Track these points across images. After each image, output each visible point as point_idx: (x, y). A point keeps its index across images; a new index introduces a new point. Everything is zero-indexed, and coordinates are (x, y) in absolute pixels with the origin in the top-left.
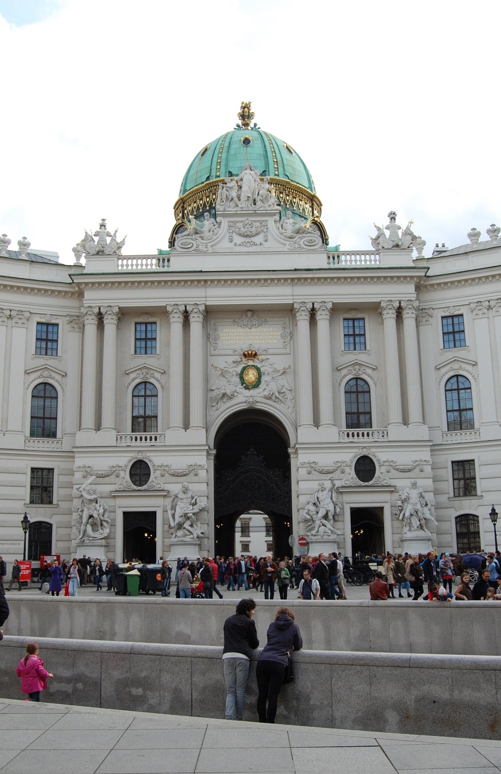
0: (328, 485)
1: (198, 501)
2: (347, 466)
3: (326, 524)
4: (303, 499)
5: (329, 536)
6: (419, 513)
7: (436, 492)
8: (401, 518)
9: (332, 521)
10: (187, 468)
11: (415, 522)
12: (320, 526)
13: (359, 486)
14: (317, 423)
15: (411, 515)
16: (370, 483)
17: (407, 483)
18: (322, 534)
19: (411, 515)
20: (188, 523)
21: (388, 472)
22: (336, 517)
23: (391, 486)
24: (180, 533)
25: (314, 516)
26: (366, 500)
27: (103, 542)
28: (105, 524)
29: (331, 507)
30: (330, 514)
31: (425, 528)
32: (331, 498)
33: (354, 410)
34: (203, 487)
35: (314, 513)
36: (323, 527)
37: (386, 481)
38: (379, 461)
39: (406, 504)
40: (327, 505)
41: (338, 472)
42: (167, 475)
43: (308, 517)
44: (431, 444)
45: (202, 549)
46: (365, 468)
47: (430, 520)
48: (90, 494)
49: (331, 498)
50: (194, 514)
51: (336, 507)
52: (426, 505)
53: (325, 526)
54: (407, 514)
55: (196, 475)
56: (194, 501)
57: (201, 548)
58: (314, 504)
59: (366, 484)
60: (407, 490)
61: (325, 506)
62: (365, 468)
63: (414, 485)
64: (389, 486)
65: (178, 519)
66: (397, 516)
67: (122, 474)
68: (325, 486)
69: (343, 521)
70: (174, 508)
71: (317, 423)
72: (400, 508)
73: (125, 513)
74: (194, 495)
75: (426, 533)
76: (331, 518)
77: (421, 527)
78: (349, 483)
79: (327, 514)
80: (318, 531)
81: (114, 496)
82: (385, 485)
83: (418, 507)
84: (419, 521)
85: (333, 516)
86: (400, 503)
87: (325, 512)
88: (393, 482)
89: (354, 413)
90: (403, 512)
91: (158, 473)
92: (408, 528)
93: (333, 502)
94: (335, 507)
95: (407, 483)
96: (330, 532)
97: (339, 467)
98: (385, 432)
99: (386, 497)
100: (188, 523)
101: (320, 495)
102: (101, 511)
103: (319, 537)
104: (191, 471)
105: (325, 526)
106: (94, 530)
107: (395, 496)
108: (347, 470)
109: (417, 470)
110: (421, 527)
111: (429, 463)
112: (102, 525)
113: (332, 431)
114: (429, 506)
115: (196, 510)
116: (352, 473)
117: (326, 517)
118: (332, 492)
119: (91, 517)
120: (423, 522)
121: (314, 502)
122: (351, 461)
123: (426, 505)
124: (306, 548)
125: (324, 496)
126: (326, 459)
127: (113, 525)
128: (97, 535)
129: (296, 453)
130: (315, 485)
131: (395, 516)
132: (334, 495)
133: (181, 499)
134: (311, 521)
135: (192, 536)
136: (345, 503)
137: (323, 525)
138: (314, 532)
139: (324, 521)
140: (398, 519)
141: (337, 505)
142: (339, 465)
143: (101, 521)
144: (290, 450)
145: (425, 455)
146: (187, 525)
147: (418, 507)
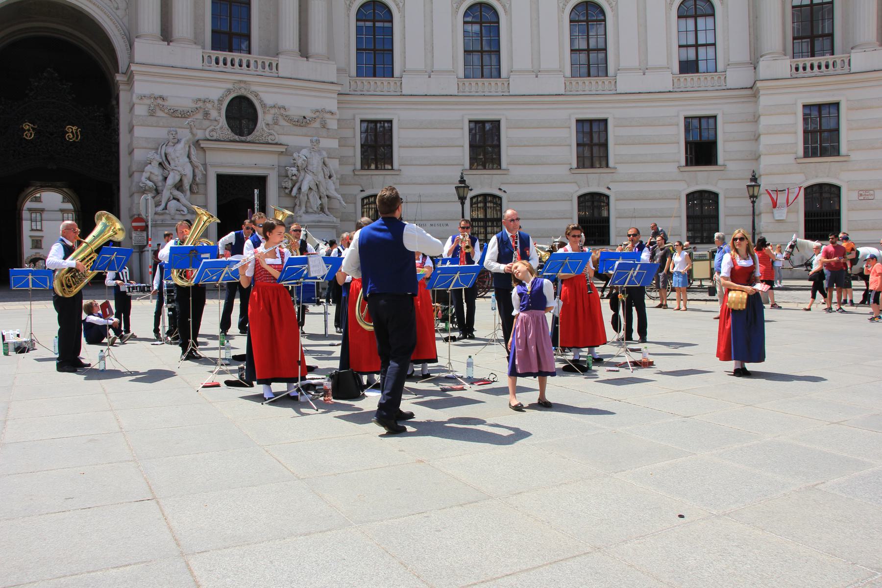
0: (185, 135)
4: (139, 155)
6: (322, 189)
7: (342, 161)
9: (188, 192)
11: (315, 202)
12: (169, 200)
14: (166, 35)
15: (310, 188)
16: (249, 138)
17: (306, 141)
19: (310, 188)
22: (195, 187)
23: (281, 144)
25: (160, 184)
29: (188, 171)
31: (326, 210)
33: (226, 29)
37: (273, 138)
38: (264, 106)
39: (302, 173)
40: (181, 166)
44: (339, 88)
46: (242, 115)
47: (335, 198)
49: (189, 157)
51: (196, 170)
52: (330, 177)
53: (178, 200)
54: (305, 188)
58: (160, 164)
59: (243, 138)
61: (180, 169)
62: (242, 115)
63: (315, 146)
64: (276, 144)
66: (287, 191)
68: (179, 137)
71: (166, 35)
72: (294, 178)
76: (188, 187)
77: (322, 209)
80: (166, 208)
82: (270, 141)
84: (320, 198)
86: (294, 170)
87: (178, 178)
88: (283, 139)
89: (224, 33)
92: (303, 208)
93: (191, 162)
94: (194, 171)
95: (306, 141)
98: (274, 65)
99: (273, 160)
101: (170, 150)
103: (168, 217)
105: (178, 200)
107: (284, 160)
108: (214, 114)
109: (317, 124)
110: (322, 209)
111: (334, 117)
113: (191, 51)
114: (334, 178)
116: (221, 120)
117: (179, 186)
121: (160, 160)
122: (220, 101)
123: (330, 177)
124: (145, 234)
125: (178, 154)
126: (181, 94)
129: (130, 81)
130: (161, 133)
137: (174, 199)
139: (177, 193)
144: (119, 78)
145: (331, 104)
147: (321, 177)
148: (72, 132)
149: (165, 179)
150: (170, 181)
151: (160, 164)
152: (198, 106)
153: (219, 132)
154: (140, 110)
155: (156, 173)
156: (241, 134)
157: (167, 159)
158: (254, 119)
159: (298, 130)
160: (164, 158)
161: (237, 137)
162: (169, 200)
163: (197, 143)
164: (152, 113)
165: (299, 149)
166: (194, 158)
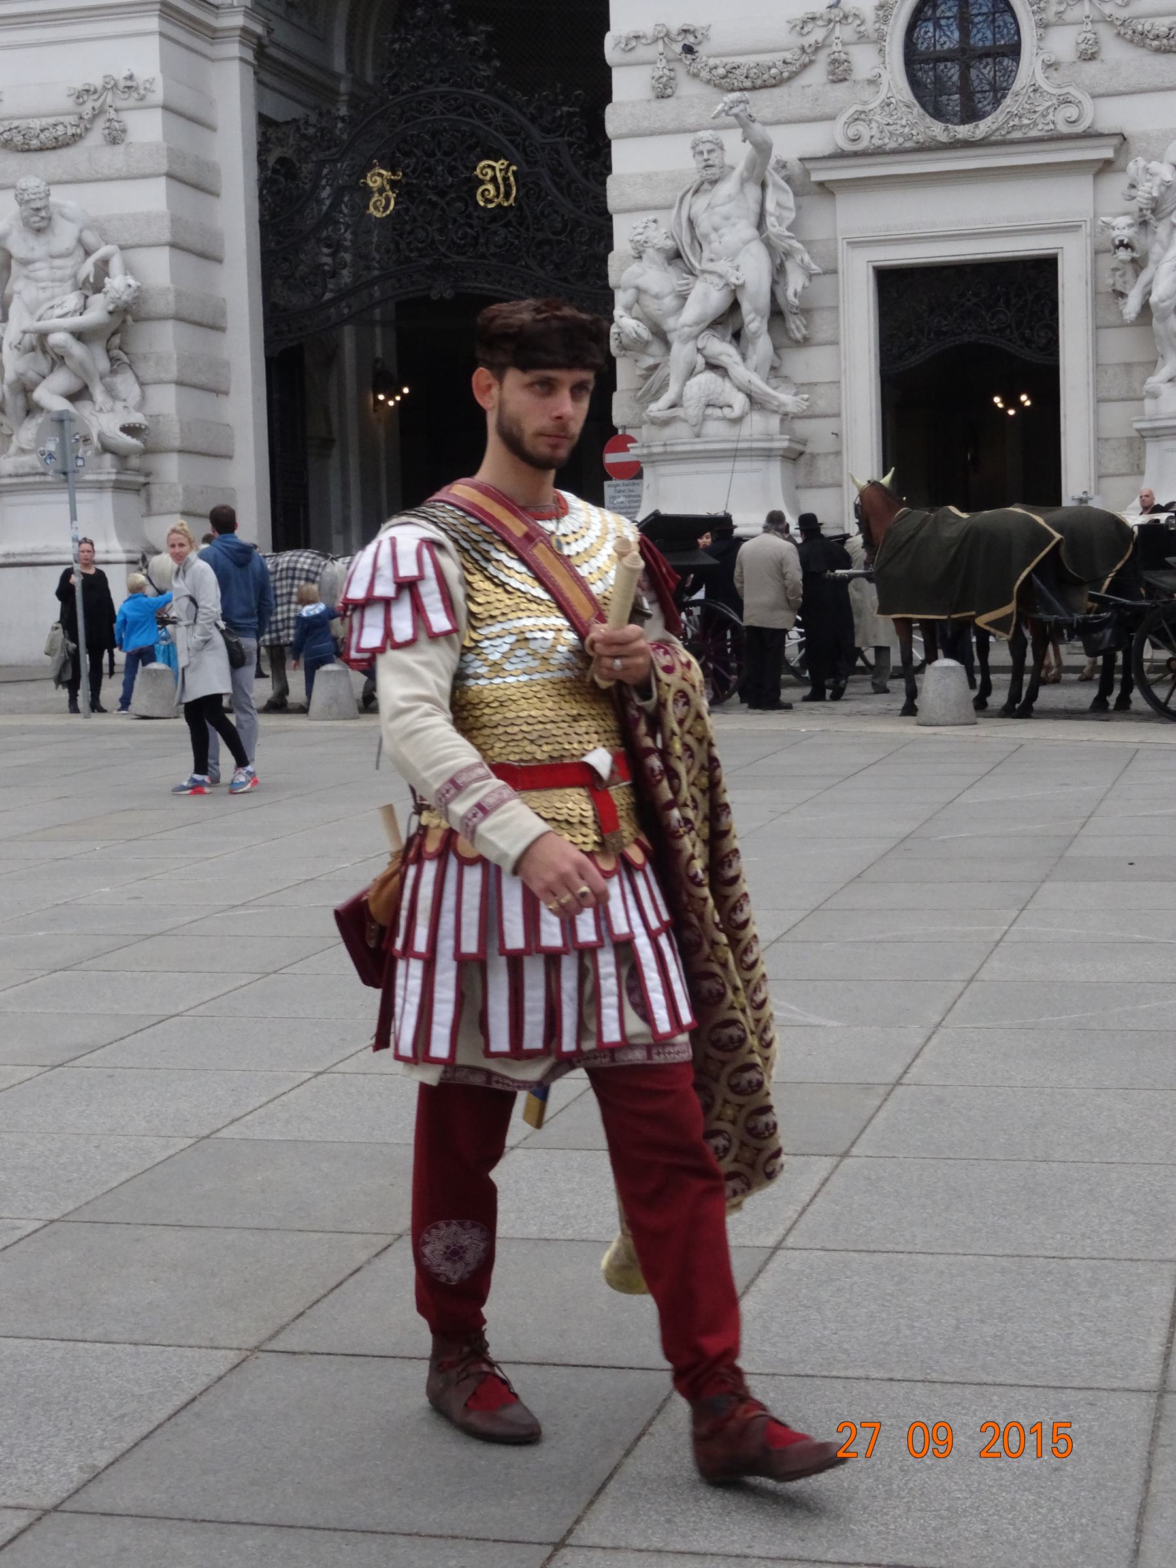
0: (737, 151)
2: (862, 38)
3: (724, 360)
5: (737, 421)
8: (1131, 306)
9: (763, 346)
10: (68, 104)
12: (691, 373)
13: (922, 148)
16: (983, 128)
18: (691, 410)
20: (61, 380)
21: (1089, 56)
25: (670, 324)
26: (963, 221)
29: (753, 271)
30: (746, 306)
32: (761, 224)
34: (151, 199)
35: (669, 302)
36: (708, 377)
37: (1072, 112)
39: (1162, 230)
41: (817, 75)
45: (155, 506)
49: (761, 224)
50: (80, 335)
51: (789, 266)
55: (115, 138)
56: (88, 268)
57: (148, 502)
59: (963, 131)
61: (722, 266)
64: (1090, 135)
69: (835, 343)
74: (90, 238)
78: (869, 135)
79: (735, 306)
82: (1064, 129)
85: (777, 314)
88: (1113, 115)
90: (1144, 277)
96: (739, 402)
97: (817, 48)
99: (1069, 199)
100: (61, 380)
104: (94, 116)
115: (97, 312)
118: (763, 186)
132: (780, 199)
133: (25, 263)
134: (656, 348)
136: (842, 246)
137: (713, 366)
138: (657, 408)
139: (721, 348)
141: (788, 254)
142: (818, 34)
148: (494, 181)
150: (692, 311)
152: (810, 40)
153: (880, 118)
154: (629, 88)
155: (655, 288)
156: (971, 115)
157: (694, 237)
158: (1014, 51)
160: (686, 238)
161: (938, 130)
164: (664, 91)
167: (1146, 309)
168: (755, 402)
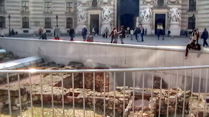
1: (110, 11)
8: (170, 17)
11: (174, 19)
12: (145, 19)
19: (173, 17)
24: (105, 20)
27: (84, 23)
28: (85, 18)
29: (149, 14)
31: (177, 21)
42: (102, 4)
43: (142, 16)
48: (80, 9)
52: (178, 13)
54: (172, 16)
55: (110, 3)
56: (109, 11)
60: (173, 9)
65: (104, 16)
67: (90, 3)
70: (103, 13)
73: (91, 15)
75: (178, 23)
81: (87, 10)
83: (176, 14)
84: (176, 18)
85: (150, 16)
88: (169, 6)
91: (100, 3)
96: (148, 21)
101: (146, 10)
102: (83, 14)
106: (82, 20)
110: (176, 21)
112: (84, 18)
115: (110, 14)
117: (147, 16)
119: (81, 16)
120: (177, 19)
123: (178, 13)
127: (87, 18)
128: (83, 21)
131: (168, 17)
132: (150, 10)
135: (108, 21)
137: (147, 19)
138: (143, 21)
139: (147, 18)
140: (169, 18)
143: (84, 17)
146: (107, 18)
149: (145, 15)
151: (144, 12)
159: (173, 4)
162: (145, 19)
163: (151, 9)
164: (143, 3)
165: (171, 8)
166: (150, 11)
167: (171, 17)
168: (149, 21)
